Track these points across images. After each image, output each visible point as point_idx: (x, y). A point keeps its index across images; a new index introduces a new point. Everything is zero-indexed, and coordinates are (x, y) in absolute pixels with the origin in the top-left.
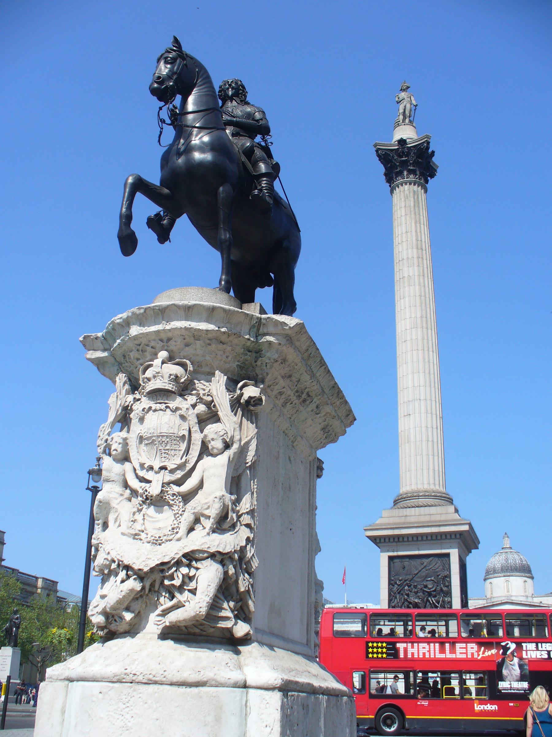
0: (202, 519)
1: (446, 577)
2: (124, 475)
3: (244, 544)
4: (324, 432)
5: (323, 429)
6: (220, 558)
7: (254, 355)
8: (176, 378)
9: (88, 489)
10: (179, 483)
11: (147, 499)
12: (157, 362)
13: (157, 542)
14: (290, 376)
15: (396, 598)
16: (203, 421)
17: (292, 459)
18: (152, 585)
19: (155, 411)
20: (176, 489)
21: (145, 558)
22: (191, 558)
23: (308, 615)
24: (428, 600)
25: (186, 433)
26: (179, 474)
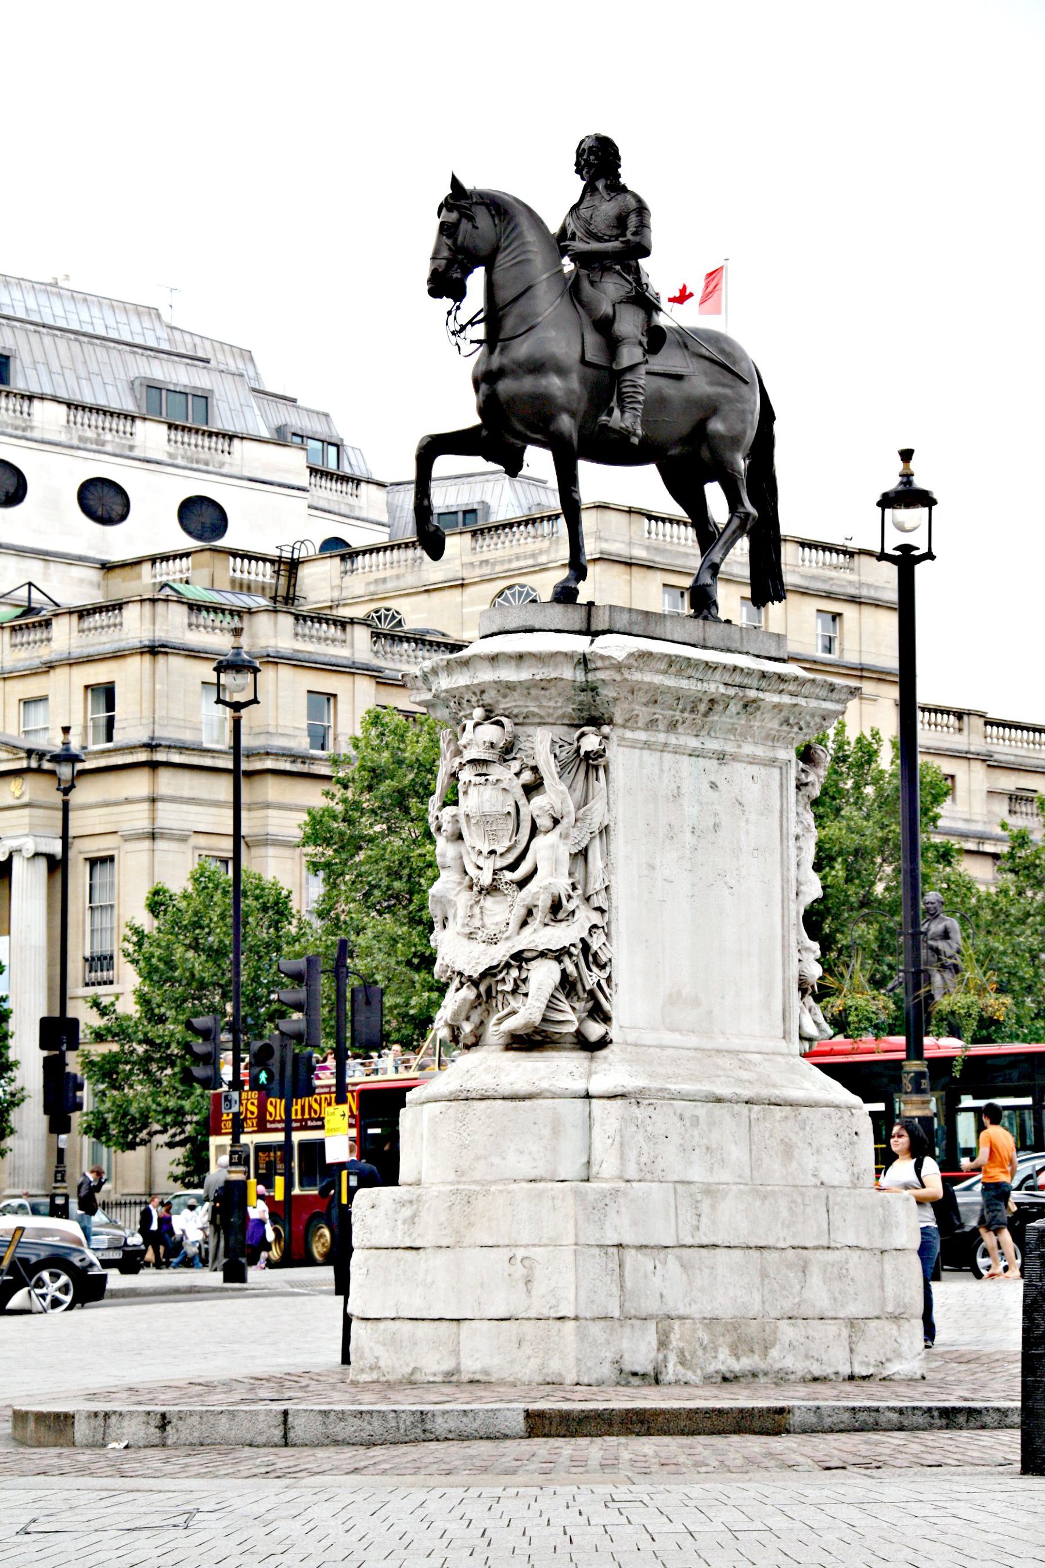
3: (585, 934)
6: (559, 955)
7: (590, 694)
10: (513, 867)
13: (493, 941)
16: (532, 789)
18: (489, 990)
20: (508, 876)
23: (784, 995)
26: (510, 859)
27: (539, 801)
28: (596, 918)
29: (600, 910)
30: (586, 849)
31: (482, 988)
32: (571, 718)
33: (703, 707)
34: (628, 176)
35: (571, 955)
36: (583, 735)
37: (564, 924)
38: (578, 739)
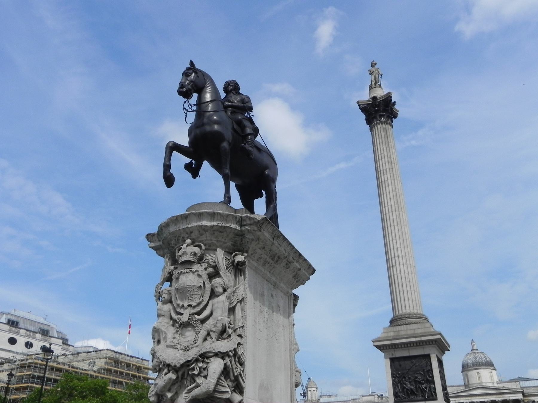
0: (211, 333)
1: (429, 370)
2: (170, 311)
3: (236, 346)
4: (295, 279)
5: (294, 277)
6: (223, 355)
8: (195, 254)
10: (199, 313)
11: (181, 324)
12: (184, 246)
13: (186, 349)
14: (264, 248)
15: (398, 386)
16: (211, 277)
17: (274, 295)
18: (183, 375)
19: (184, 273)
22: (204, 357)
23: (291, 390)
24: (419, 387)
25: (202, 285)
26: (198, 309)
27: (217, 281)
28: (239, 340)
29: (240, 336)
30: (234, 308)
31: (180, 373)
33: (276, 258)
35: (229, 356)
36: (236, 255)
37: (226, 340)
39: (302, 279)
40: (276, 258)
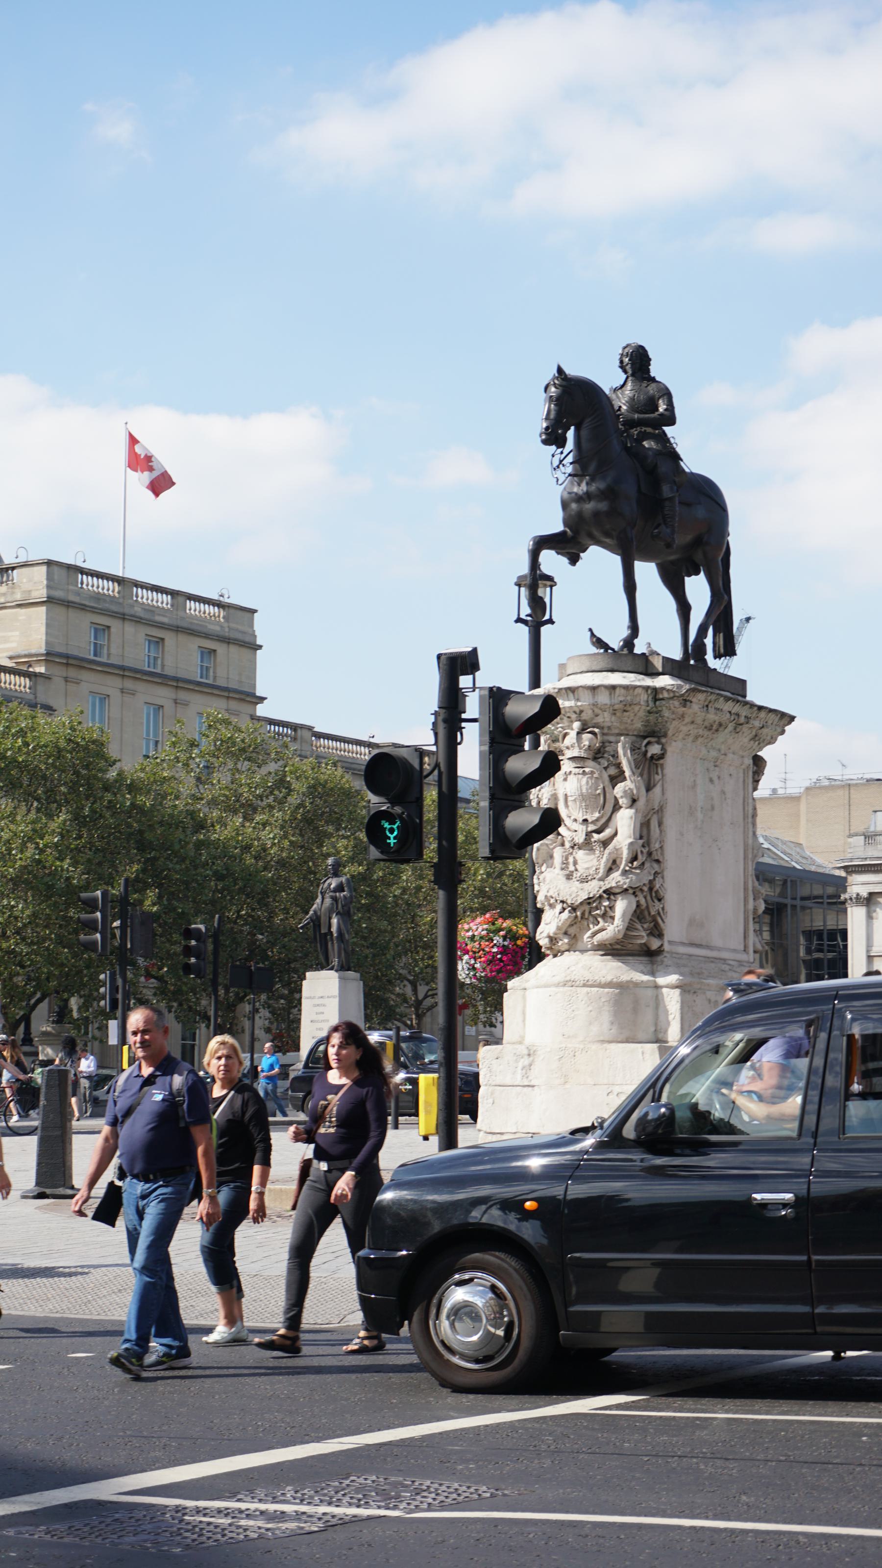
3: (651, 878)
9: (519, 620)
10: (598, 831)
13: (584, 880)
14: (693, 722)
17: (715, 779)
18: (583, 914)
20: (596, 836)
21: (578, 892)
22: (609, 893)
29: (658, 861)
30: (649, 820)
32: (640, 731)
33: (715, 727)
34: (655, 371)
35: (642, 890)
36: (649, 743)
38: (646, 746)
39: (769, 738)
40: (715, 727)
